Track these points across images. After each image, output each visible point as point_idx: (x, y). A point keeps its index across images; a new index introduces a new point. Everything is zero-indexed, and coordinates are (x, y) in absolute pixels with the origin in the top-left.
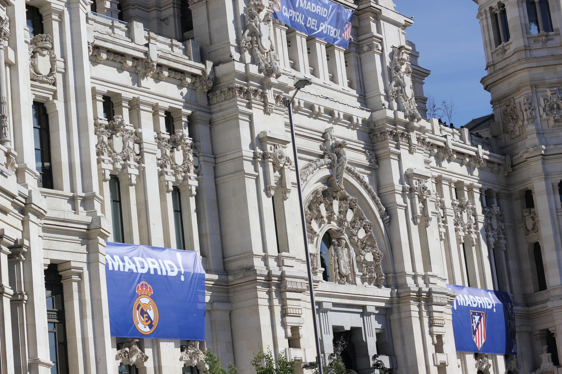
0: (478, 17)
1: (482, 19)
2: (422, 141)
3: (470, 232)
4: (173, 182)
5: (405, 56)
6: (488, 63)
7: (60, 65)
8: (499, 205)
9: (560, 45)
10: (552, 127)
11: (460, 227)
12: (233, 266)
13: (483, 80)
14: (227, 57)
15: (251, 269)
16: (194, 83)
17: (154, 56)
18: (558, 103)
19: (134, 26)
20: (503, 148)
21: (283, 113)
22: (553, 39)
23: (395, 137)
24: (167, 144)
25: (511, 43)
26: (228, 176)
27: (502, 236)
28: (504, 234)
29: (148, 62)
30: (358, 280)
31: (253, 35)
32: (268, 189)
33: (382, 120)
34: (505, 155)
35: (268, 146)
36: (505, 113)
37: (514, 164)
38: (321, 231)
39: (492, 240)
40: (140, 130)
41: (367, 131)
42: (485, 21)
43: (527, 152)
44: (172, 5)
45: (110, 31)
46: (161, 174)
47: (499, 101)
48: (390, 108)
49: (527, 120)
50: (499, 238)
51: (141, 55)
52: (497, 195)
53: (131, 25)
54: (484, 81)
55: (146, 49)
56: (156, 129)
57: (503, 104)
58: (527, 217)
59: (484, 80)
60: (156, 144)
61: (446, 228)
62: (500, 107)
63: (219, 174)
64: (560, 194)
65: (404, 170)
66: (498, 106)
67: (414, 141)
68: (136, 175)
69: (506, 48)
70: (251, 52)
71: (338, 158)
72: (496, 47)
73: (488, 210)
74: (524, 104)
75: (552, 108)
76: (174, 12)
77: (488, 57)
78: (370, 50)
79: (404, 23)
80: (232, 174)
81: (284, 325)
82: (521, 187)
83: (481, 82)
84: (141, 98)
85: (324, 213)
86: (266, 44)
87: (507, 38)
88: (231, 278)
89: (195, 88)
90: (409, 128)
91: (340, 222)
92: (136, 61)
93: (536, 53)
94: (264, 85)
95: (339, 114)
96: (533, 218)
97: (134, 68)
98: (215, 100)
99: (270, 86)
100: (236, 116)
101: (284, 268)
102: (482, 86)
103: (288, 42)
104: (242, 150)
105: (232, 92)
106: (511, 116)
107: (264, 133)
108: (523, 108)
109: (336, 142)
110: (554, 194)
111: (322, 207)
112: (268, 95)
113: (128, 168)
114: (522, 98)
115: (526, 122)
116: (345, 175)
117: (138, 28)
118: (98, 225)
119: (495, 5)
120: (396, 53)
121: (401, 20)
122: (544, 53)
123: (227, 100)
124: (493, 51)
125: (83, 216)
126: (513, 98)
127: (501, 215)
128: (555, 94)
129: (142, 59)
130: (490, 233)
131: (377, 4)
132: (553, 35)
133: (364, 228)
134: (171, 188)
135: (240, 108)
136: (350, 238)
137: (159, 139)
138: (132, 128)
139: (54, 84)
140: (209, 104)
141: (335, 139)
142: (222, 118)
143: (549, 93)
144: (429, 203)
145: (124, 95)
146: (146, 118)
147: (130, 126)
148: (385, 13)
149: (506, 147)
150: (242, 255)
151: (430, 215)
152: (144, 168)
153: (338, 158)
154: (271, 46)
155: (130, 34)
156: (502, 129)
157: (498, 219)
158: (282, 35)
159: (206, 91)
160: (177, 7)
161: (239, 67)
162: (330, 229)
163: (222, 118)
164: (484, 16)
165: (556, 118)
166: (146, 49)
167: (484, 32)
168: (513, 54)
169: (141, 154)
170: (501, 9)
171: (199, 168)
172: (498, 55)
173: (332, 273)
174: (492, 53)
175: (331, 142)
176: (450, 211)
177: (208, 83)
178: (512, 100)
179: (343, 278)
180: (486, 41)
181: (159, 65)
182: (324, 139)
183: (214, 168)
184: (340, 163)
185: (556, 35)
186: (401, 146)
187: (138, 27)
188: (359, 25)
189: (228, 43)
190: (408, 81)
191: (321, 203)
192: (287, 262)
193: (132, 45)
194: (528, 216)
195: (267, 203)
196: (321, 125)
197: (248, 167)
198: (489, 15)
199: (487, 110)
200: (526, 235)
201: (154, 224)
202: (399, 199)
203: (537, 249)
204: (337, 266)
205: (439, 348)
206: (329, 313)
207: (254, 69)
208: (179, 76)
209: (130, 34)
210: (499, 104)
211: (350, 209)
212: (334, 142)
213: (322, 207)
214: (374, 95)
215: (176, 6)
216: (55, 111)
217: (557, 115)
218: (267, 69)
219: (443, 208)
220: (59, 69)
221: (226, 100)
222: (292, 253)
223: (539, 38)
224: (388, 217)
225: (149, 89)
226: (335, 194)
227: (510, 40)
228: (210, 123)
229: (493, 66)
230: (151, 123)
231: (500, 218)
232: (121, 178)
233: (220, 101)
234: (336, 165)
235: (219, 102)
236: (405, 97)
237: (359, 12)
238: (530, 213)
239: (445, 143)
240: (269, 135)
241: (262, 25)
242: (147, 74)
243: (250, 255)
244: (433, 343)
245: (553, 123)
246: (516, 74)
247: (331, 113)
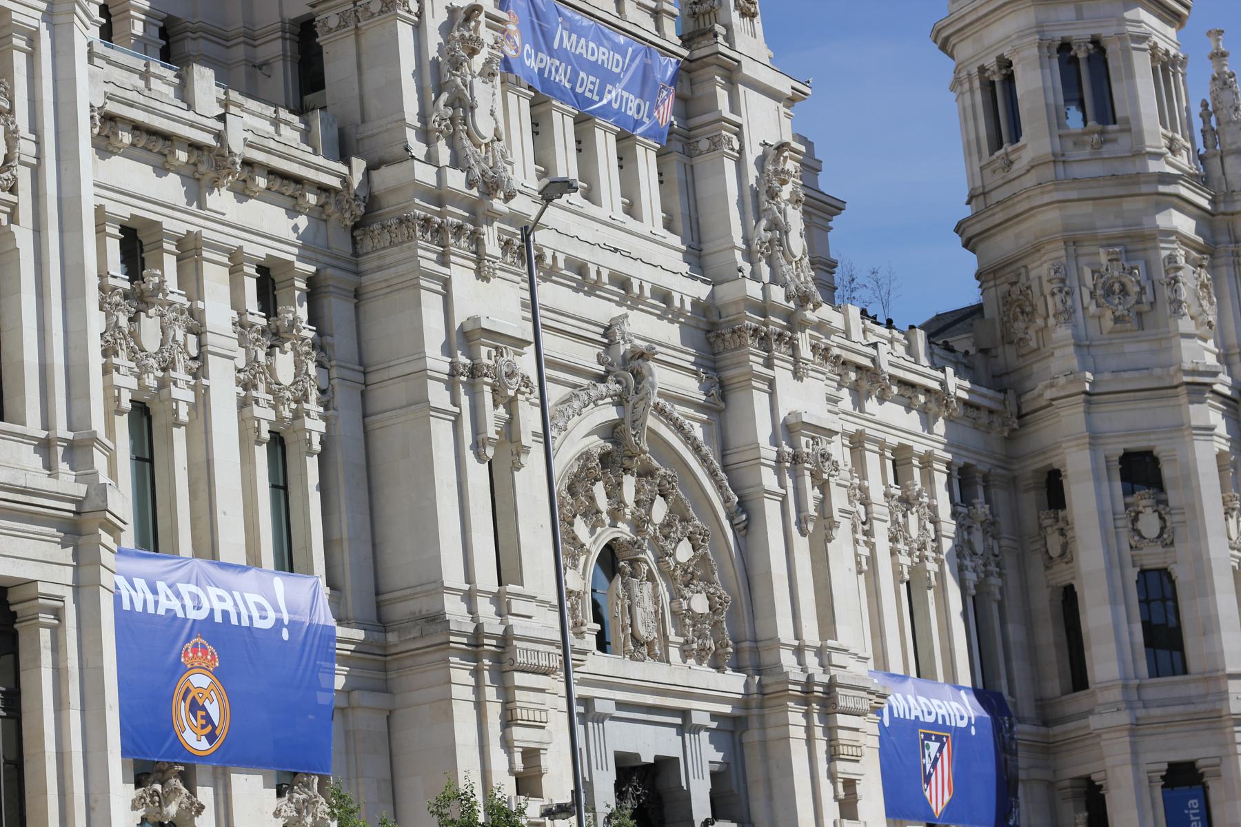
0: (952, 89)
1: (962, 93)
2: (823, 353)
3: (923, 559)
4: (270, 422)
5: (791, 166)
6: (972, 189)
7: (26, 148)
8: (988, 501)
9: (1130, 154)
10: (1110, 333)
11: (901, 546)
12: (399, 611)
13: (961, 224)
14: (398, 150)
15: (438, 619)
16: (322, 206)
17: (236, 142)
18: (1124, 280)
19: (195, 77)
20: (1000, 376)
21: (518, 279)
22: (1114, 141)
23: (764, 341)
24: (260, 337)
25: (1024, 146)
26: (393, 413)
27: (993, 568)
28: (998, 565)
29: (223, 156)
30: (674, 653)
31: (457, 104)
32: (481, 444)
33: (736, 303)
34: (1004, 391)
35: (484, 351)
36: (1006, 300)
37: (1024, 411)
38: (595, 542)
39: (971, 577)
40: (200, 305)
41: (702, 326)
42: (968, 96)
43: (1052, 386)
44: (280, 34)
45: (141, 84)
46: (243, 404)
47: (995, 272)
48: (755, 276)
49: (1055, 316)
50: (988, 574)
51: (208, 139)
52: (986, 478)
53: (187, 72)
54: (962, 229)
55: (219, 126)
56: (237, 303)
57: (1003, 279)
58: (1049, 530)
59: (963, 226)
60: (236, 336)
61: (872, 547)
62: (995, 285)
63: (371, 408)
64: (1123, 479)
65: (782, 414)
66: (992, 283)
67: (806, 352)
68: (188, 403)
69: (1012, 157)
70: (452, 142)
71: (638, 383)
72: (991, 154)
73: (965, 510)
74: (1050, 281)
75: (1109, 292)
76: (284, 49)
77: (973, 175)
78: (714, 150)
79: (789, 92)
80: (401, 408)
81: (507, 744)
82: (1039, 463)
83: (957, 230)
84: (205, 233)
85: (602, 502)
86: (484, 125)
87: (1016, 134)
88: (392, 638)
89: (324, 217)
90: (794, 322)
91: (639, 525)
92: (196, 153)
93: (1077, 171)
94: (479, 214)
95: (641, 287)
96: (1062, 532)
97: (193, 168)
98: (368, 244)
99: (491, 217)
100: (415, 282)
101: (512, 620)
102: (958, 240)
103: (535, 124)
104: (425, 357)
105: (407, 227)
106: (1020, 306)
107: (476, 320)
108: (1047, 289)
109: (636, 346)
110: (1110, 480)
111: (599, 490)
112: (486, 238)
113: (173, 387)
114: (1046, 266)
115: (1051, 321)
116: (652, 422)
117: (204, 80)
118: (101, 504)
119: (990, 62)
120: (770, 158)
121: (784, 85)
122: (1095, 169)
123: (395, 245)
124: (984, 162)
125: (67, 482)
126: (1025, 267)
127: (993, 524)
128: (1117, 260)
129: (209, 148)
130: (967, 562)
131: (732, 48)
132: (1115, 132)
133: (689, 538)
134: (266, 436)
135: (423, 263)
136: (658, 560)
137: (242, 326)
138: (184, 300)
139: (13, 190)
140: (356, 254)
141: (631, 341)
142: (384, 285)
143: (1103, 259)
144: (834, 489)
145: (168, 224)
146: (215, 278)
147: (179, 294)
148: (749, 69)
149: (1008, 373)
150: (419, 589)
151: (836, 515)
152: (207, 388)
153: (638, 383)
154: (496, 129)
155: (184, 92)
156: (999, 336)
157: (985, 532)
158: (520, 108)
159: (350, 223)
160: (290, 39)
161: (425, 174)
162: (615, 539)
163: (384, 285)
164: (966, 86)
165: (1117, 314)
166: (219, 126)
167: (966, 121)
168: (1028, 171)
169: (201, 356)
170: (1004, 71)
171: (330, 393)
172: (994, 172)
173: (617, 635)
174: (981, 168)
175: (623, 348)
176: (880, 508)
177: (354, 204)
178: (1023, 270)
179: (640, 647)
180: (968, 142)
181: (247, 163)
182: (606, 341)
183: (363, 394)
184: (641, 394)
185: (1121, 131)
186: (776, 362)
187: (202, 77)
188: (692, 93)
189: (400, 120)
190: (795, 219)
191: (597, 480)
192: (517, 606)
193: (189, 115)
194: (1051, 526)
195: (478, 475)
196: (602, 310)
197: (438, 395)
198: (977, 84)
199: (967, 294)
200: (1047, 568)
201: (225, 513)
202: (769, 479)
203: (1069, 599)
204: (628, 621)
206: (607, 723)
207: (456, 180)
208: (290, 189)
209: (184, 92)
210: (995, 279)
211: (661, 495)
212: (628, 346)
213: (599, 490)
214: (721, 248)
215: (288, 35)
216: (12, 250)
217: (1120, 307)
218: (486, 180)
219: (866, 502)
220: (23, 158)
221: (392, 244)
222: (528, 589)
223: (1087, 138)
224: (744, 517)
225: (224, 214)
226: (627, 463)
227: (1023, 140)
228: (357, 294)
229: (982, 196)
230: (226, 289)
231: (991, 528)
232: (155, 409)
233: (379, 247)
234: (633, 399)
235: (377, 250)
236: (788, 254)
237: (693, 64)
238: (1057, 520)
239: (873, 360)
240: (485, 324)
241: (477, 82)
242: (220, 182)
243: (437, 588)
244: (836, 798)
245: (1112, 323)
246: (1033, 215)
247: (623, 282)
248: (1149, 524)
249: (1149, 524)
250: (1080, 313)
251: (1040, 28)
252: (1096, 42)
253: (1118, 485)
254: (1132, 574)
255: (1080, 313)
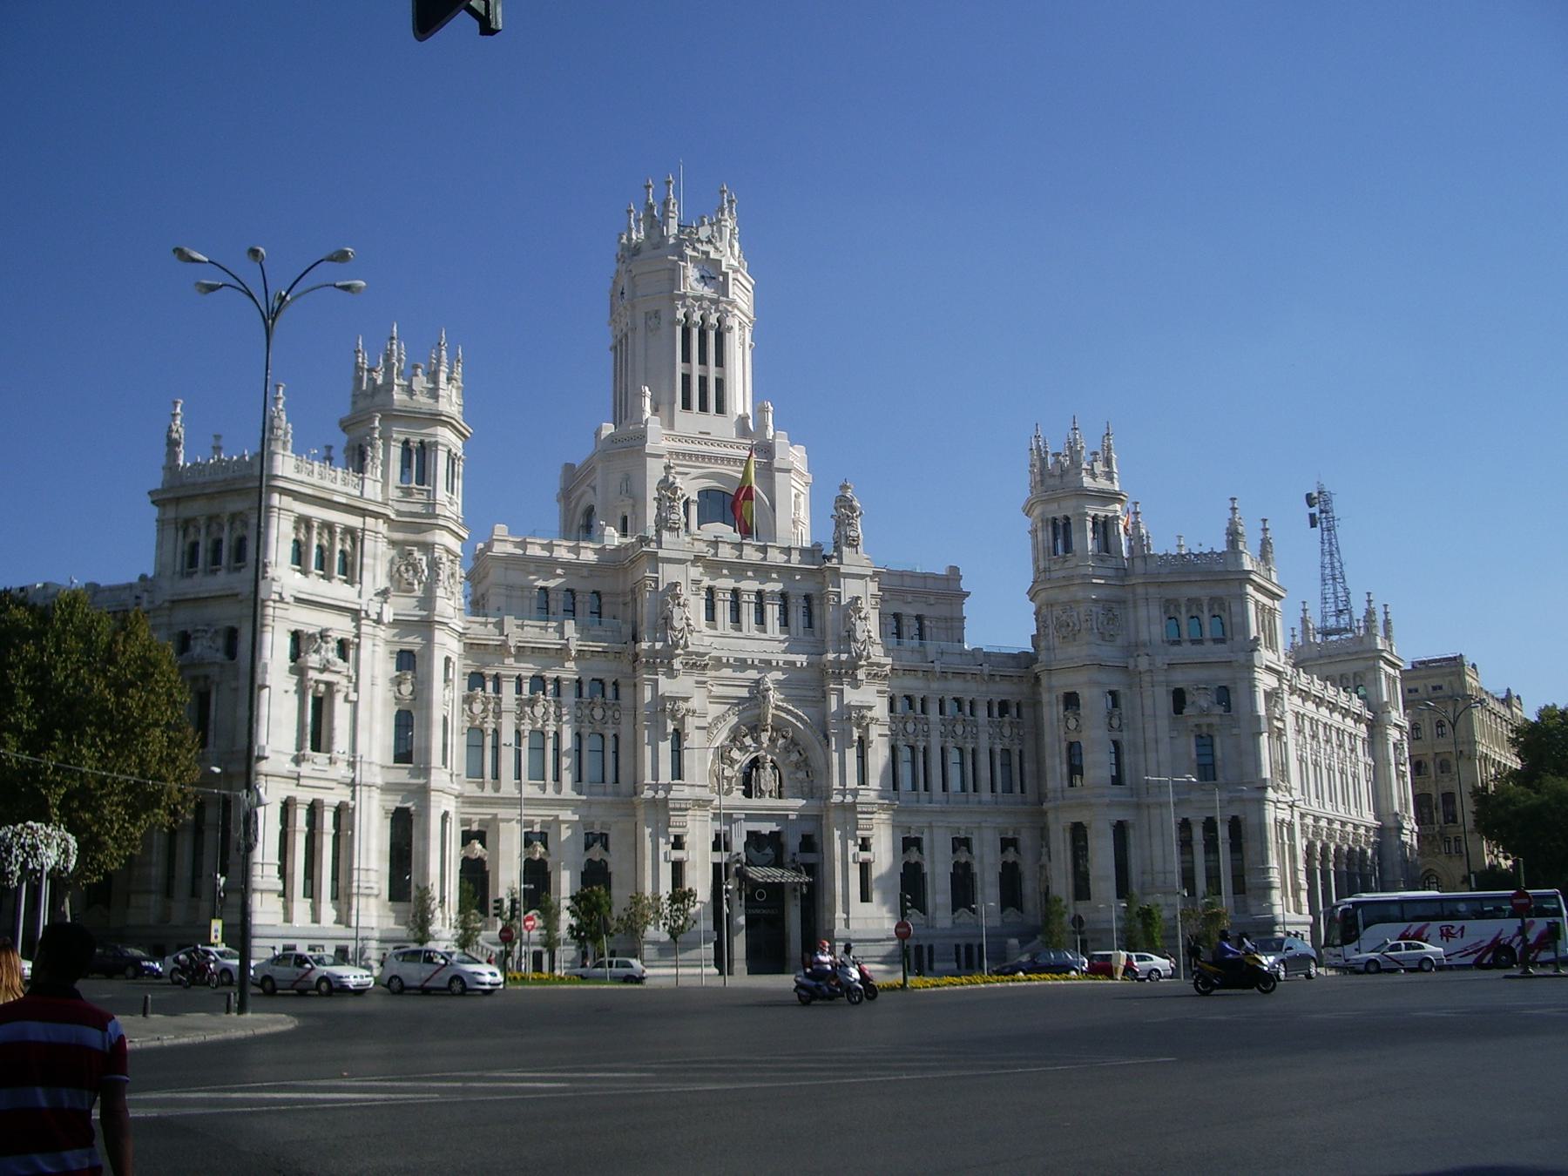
93: (1054, 575)
110: (1058, 705)
122: (1061, 574)
196: (753, 674)
205: (865, 846)
248: (1072, 724)
249: (1072, 724)
250: (1051, 636)
251: (1043, 513)
252: (1067, 518)
253: (1061, 708)
254: (1064, 745)
255: (1051, 636)
